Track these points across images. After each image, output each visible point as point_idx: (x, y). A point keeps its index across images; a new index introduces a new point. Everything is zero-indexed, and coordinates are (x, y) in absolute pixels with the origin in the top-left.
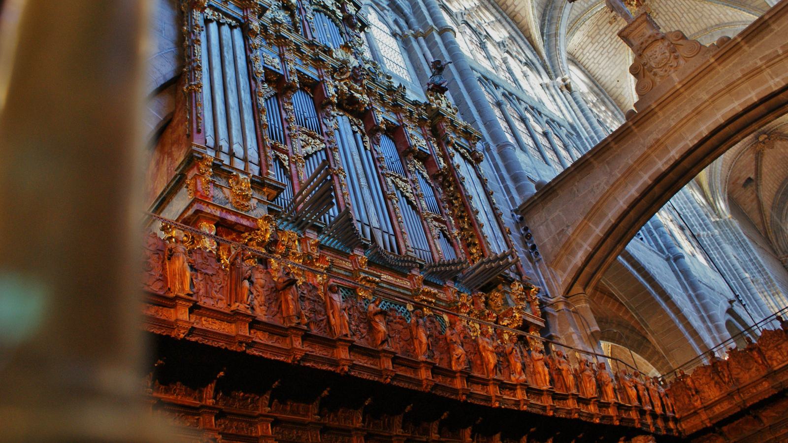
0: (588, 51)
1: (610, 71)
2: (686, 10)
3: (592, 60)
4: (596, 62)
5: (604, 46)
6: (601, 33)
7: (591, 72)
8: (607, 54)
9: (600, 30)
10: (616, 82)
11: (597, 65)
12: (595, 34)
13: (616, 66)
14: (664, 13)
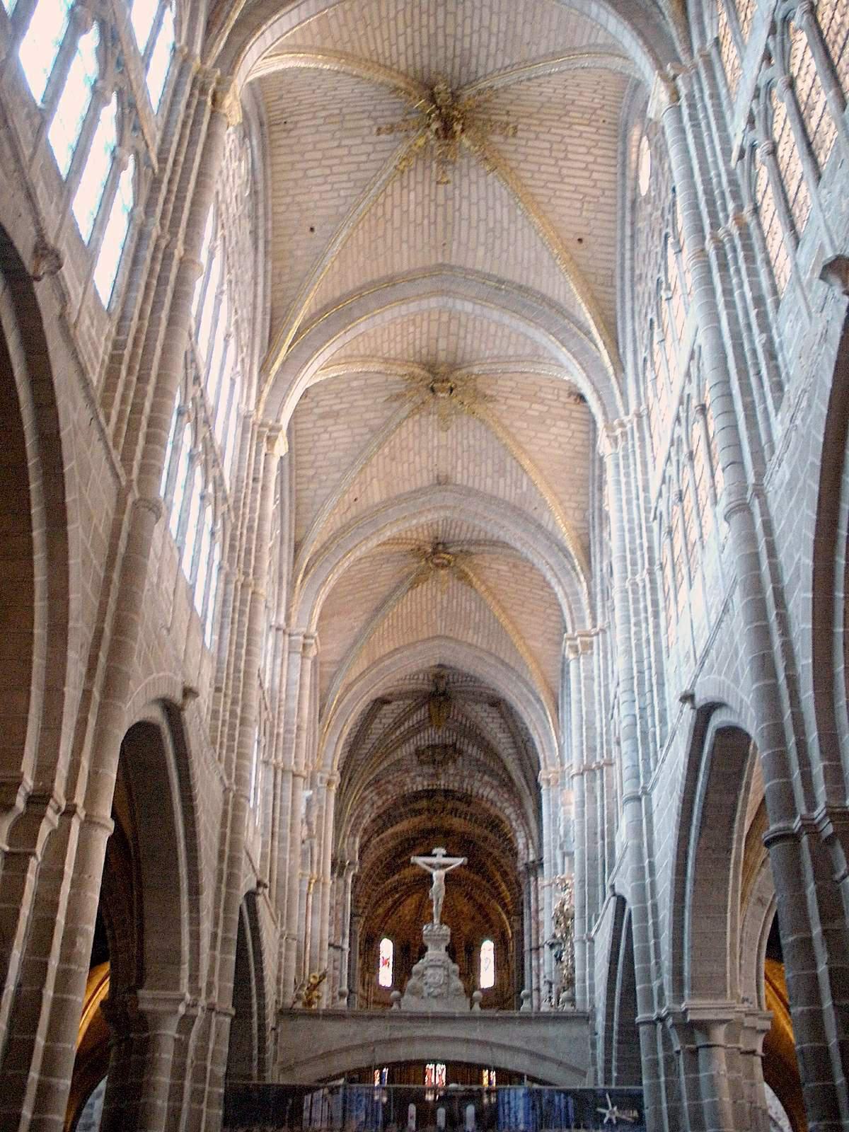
14: (424, 30)
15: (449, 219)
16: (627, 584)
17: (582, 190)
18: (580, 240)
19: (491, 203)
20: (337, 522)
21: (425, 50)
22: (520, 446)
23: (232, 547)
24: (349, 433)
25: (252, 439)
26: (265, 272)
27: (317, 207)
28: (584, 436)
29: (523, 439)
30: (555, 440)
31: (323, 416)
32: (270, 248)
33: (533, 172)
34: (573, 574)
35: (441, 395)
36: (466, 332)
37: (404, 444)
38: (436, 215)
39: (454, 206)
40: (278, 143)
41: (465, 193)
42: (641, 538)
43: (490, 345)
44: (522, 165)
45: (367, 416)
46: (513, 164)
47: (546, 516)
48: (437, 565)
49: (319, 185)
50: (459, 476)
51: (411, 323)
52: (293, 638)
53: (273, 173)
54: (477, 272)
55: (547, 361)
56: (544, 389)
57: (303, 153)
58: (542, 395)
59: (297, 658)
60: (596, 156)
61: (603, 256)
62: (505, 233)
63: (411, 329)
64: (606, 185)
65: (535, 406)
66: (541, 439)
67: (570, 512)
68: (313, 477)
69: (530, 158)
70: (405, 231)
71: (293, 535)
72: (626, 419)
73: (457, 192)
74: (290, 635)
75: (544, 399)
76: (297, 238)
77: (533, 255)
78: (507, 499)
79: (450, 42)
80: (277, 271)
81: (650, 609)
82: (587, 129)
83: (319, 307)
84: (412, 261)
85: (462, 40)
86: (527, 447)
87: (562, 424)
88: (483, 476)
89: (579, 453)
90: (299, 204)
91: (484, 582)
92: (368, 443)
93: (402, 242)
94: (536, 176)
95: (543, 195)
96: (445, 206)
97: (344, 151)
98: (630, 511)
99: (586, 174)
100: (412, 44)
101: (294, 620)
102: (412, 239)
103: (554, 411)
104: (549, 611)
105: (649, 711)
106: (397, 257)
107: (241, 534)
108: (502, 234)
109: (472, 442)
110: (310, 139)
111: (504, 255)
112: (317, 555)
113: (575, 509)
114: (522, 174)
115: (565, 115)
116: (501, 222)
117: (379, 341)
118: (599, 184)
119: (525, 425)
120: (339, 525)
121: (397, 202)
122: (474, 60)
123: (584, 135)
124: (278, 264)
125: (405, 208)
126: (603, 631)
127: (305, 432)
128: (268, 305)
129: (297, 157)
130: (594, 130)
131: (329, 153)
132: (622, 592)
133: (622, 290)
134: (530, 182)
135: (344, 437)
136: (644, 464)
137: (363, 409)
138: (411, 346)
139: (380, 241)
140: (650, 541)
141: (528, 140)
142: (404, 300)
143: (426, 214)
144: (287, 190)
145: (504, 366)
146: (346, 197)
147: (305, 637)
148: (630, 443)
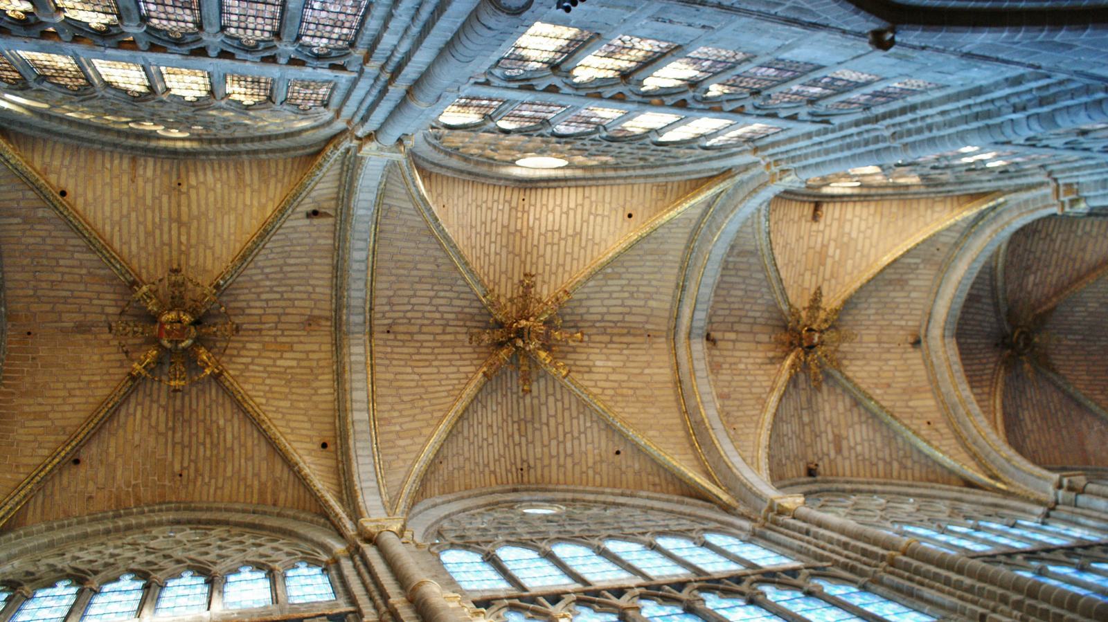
0: (502, 210)
2: (425, 384)
4: (484, 205)
5: (488, 237)
6: (504, 250)
7: (480, 187)
8: (478, 230)
9: (509, 253)
11: (479, 203)
12: (511, 242)
14: (436, 351)
15: (625, 331)
16: (897, 144)
18: (630, 216)
19: (606, 296)
20: (950, 442)
21: (456, 350)
23: (852, 569)
24: (857, 427)
25: (774, 530)
26: (648, 498)
27: (599, 447)
29: (864, 264)
31: (839, 450)
32: (628, 492)
33: (573, 259)
34: (999, 209)
35: (816, 339)
36: (746, 316)
37: (874, 375)
38: (621, 343)
39: (612, 327)
40: (539, 477)
41: (599, 317)
42: (851, 135)
43: (758, 295)
44: (568, 268)
45: (841, 407)
47: (942, 239)
48: (1026, 345)
49: (580, 445)
50: (910, 323)
51: (733, 367)
52: (1060, 501)
53: (565, 484)
54: (671, 307)
55: (758, 243)
56: (812, 244)
57: (551, 457)
59: (1082, 499)
60: (555, 205)
61: (642, 195)
62: (632, 283)
63: (742, 366)
65: (831, 252)
66: (863, 246)
67: (936, 216)
68: (900, 463)
69: (561, 262)
70: (631, 371)
71: (956, 488)
72: (763, 163)
73: (598, 324)
74: (1057, 503)
75: (822, 245)
76: (624, 468)
77: (649, 257)
80: (651, 487)
81: (910, 116)
83: (690, 451)
84: (661, 364)
85: (448, 320)
88: (909, 300)
90: (595, 463)
91: (1048, 299)
92: (867, 409)
94: (576, 256)
96: (612, 335)
97: (552, 422)
98: (834, 150)
99: (571, 213)
101: (1043, 497)
103: (834, 235)
104: (1079, 233)
105: (1014, 100)
106: (656, 378)
107: (847, 557)
109: (873, 311)
110: (538, 450)
111: (654, 283)
112: (983, 466)
113: (933, 212)
115: (521, 233)
116: (623, 286)
117: (749, 396)
118: (580, 201)
119: (850, 262)
120: (954, 441)
121: (604, 377)
122: (467, 310)
123: (537, 216)
124: (645, 485)
125: (610, 370)
126: (1050, 174)
127: (854, 468)
128: (676, 498)
129: (554, 461)
130: (532, 208)
131: (553, 435)
132: (905, 150)
133: (666, 175)
135: (861, 432)
136: (791, 140)
137: (834, 413)
138: (764, 367)
139: (637, 392)
140: (850, 125)
141: (545, 264)
142: (693, 372)
144: (582, 472)
145: (774, 282)
146: (592, 422)
147: (1060, 486)
148: (780, 157)
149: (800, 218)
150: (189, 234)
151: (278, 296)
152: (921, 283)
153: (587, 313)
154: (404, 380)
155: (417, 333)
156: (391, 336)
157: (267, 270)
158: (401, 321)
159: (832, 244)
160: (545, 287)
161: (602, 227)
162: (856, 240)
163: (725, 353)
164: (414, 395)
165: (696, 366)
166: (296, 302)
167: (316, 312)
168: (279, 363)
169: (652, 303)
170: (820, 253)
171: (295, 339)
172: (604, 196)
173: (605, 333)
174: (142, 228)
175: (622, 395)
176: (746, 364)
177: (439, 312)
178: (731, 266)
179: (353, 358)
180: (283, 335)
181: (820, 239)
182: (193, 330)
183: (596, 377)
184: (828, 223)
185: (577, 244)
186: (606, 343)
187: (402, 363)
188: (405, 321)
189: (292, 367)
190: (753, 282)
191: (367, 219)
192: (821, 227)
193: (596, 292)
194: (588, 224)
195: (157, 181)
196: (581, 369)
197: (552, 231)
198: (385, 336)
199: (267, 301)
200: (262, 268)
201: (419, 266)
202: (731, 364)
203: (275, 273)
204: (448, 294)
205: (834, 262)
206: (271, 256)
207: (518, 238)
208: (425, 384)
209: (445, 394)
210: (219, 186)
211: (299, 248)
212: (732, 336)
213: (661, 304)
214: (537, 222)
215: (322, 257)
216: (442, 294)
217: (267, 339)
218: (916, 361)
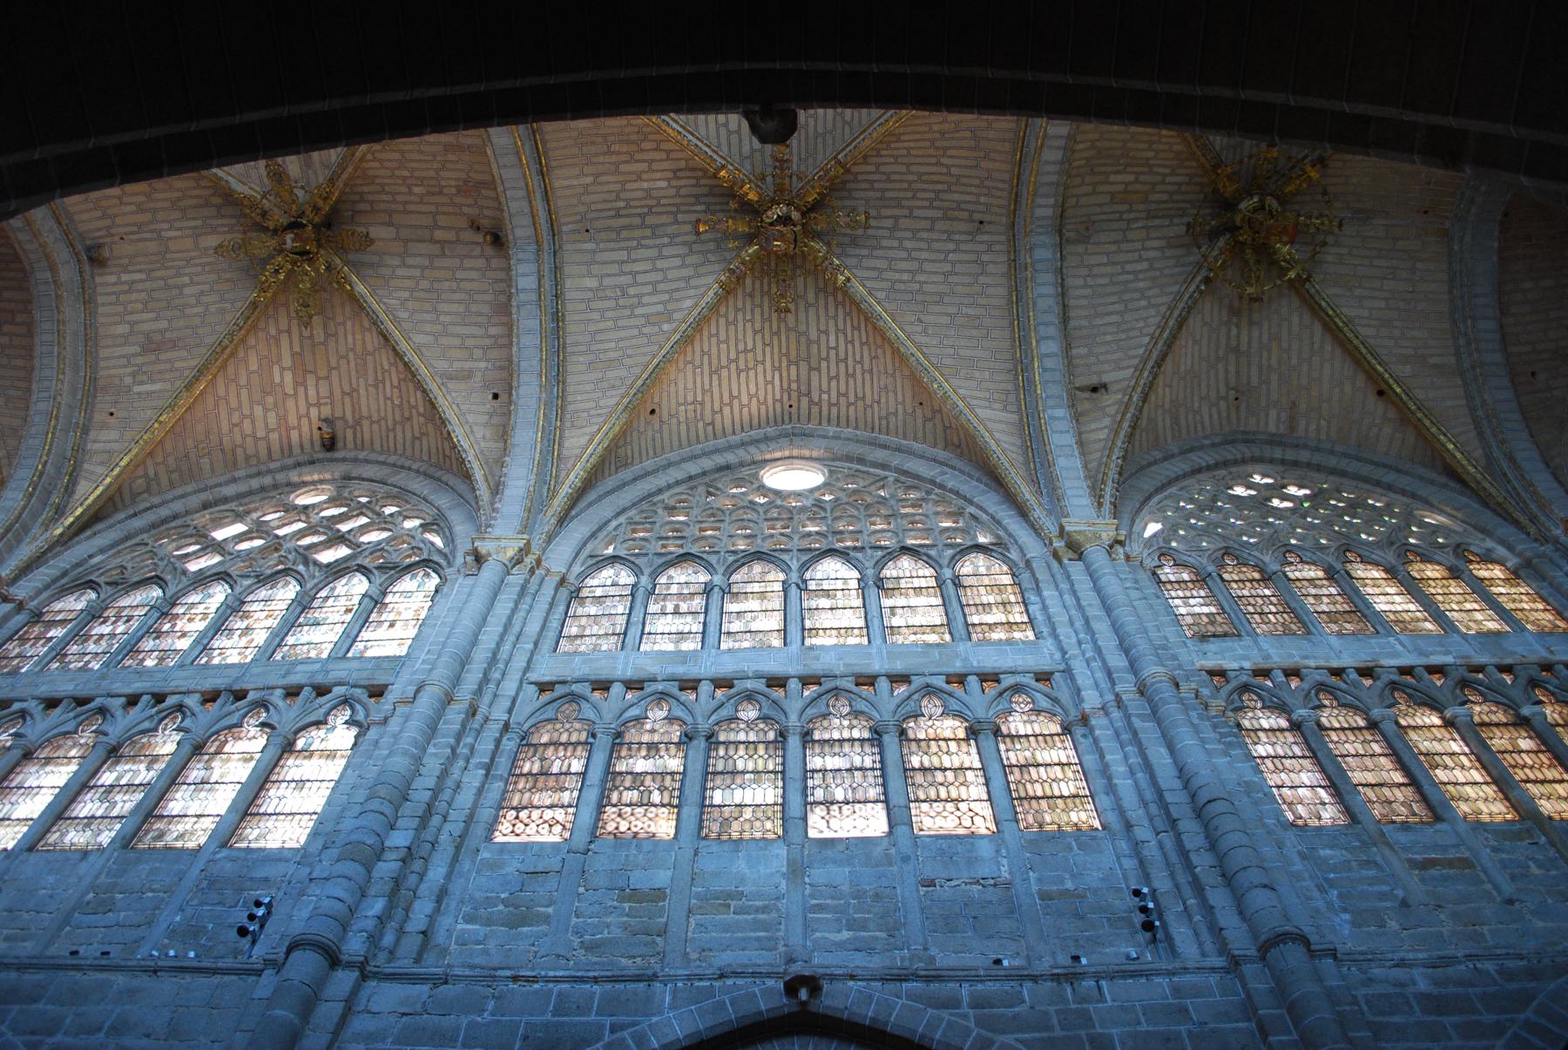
1: (891, 395)
2: (932, 152)
3: (843, 400)
4: (852, 399)
5: (842, 355)
6: (813, 335)
8: (858, 367)
9: (806, 333)
10: (919, 412)
11: (860, 403)
12: (803, 348)
13: (893, 376)
14: (910, 195)
15: (624, 234)
17: (708, 399)
18: (653, 412)
19: (661, 287)
21: (878, 194)
22: (223, 367)
28: (263, 453)
30: (245, 417)
33: (717, 334)
34: (48, 513)
41: (665, 252)
43: (410, 304)
44: (722, 321)
46: (723, 310)
50: (113, 279)
58: (311, 381)
60: (749, 405)
64: (718, 426)
65: (288, 377)
66: (239, 395)
69: (732, 328)
73: (666, 240)
77: (613, 355)
78: (102, 364)
79: (889, 223)
82: (777, 388)
84: (568, 192)
86: (220, 381)
87: (272, 419)
88: (128, 318)
89: (234, 454)
93: (597, 176)
94: (714, 340)
95: (693, 352)
96: (643, 226)
99: (726, 399)
100: (891, 181)
102: (599, 188)
103: (290, 403)
106: (576, 171)
108: (624, 307)
111: (596, 316)
114: (713, 323)
115: (789, 361)
118: (718, 416)
119: (254, 366)
121: (655, 166)
122: (865, 252)
123: (769, 387)
125: (645, 176)
130: (778, 397)
134: (705, 333)
139: (605, 149)
141: (752, 321)
143: (632, 203)
149: (358, 422)
150: (1229, 338)
151: (1129, 267)
152: (118, 351)
153: (683, 257)
154: (966, 158)
155: (938, 219)
156: (978, 217)
157: (1143, 303)
158: (963, 237)
159: (290, 390)
160: (749, 289)
161: (685, 388)
162: (252, 403)
163: (451, 210)
164: (953, 138)
165: (525, 204)
166: (1105, 260)
167: (1080, 249)
168: (1131, 178)
169: (591, 283)
170: (305, 371)
171: (1106, 209)
172: (688, 429)
173: (654, 227)
174: (1285, 345)
175: (629, 142)
176: (410, 193)
177: (906, 249)
178: (478, 353)
179: (1052, 201)
180: (1121, 213)
181: (312, 392)
182: (1238, 221)
183: (666, 165)
184: (305, 421)
185: (714, 357)
186: (650, 212)
187: (964, 181)
188: (957, 237)
189: (1117, 173)
190: (428, 327)
191: (1050, 402)
192: (314, 412)
193: (677, 290)
194: (703, 389)
195: (1263, 403)
196: (689, 174)
197: (748, 369)
198: (987, 218)
199: (1141, 259)
200: (1151, 306)
201: (945, 320)
202: (440, 193)
203: (1133, 300)
204: (897, 276)
205: (279, 360)
206: (1141, 324)
207: (793, 353)
208: (932, 152)
209: (903, 138)
210: (1196, 405)
211: (1109, 338)
212: (439, 234)
213: (578, 283)
214: (769, 378)
215: (1080, 328)
216: (905, 277)
217: (1141, 207)
218: (85, 216)
